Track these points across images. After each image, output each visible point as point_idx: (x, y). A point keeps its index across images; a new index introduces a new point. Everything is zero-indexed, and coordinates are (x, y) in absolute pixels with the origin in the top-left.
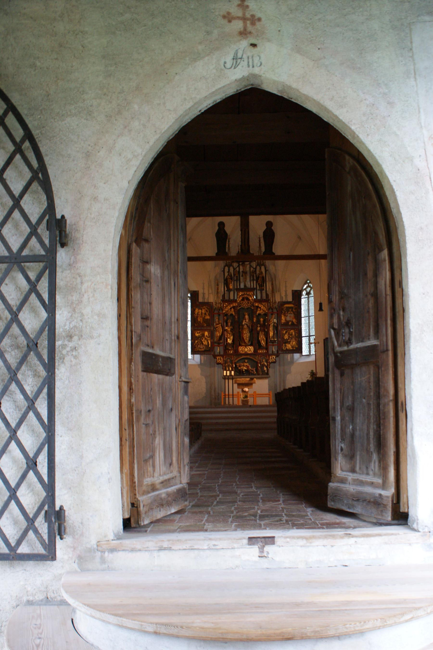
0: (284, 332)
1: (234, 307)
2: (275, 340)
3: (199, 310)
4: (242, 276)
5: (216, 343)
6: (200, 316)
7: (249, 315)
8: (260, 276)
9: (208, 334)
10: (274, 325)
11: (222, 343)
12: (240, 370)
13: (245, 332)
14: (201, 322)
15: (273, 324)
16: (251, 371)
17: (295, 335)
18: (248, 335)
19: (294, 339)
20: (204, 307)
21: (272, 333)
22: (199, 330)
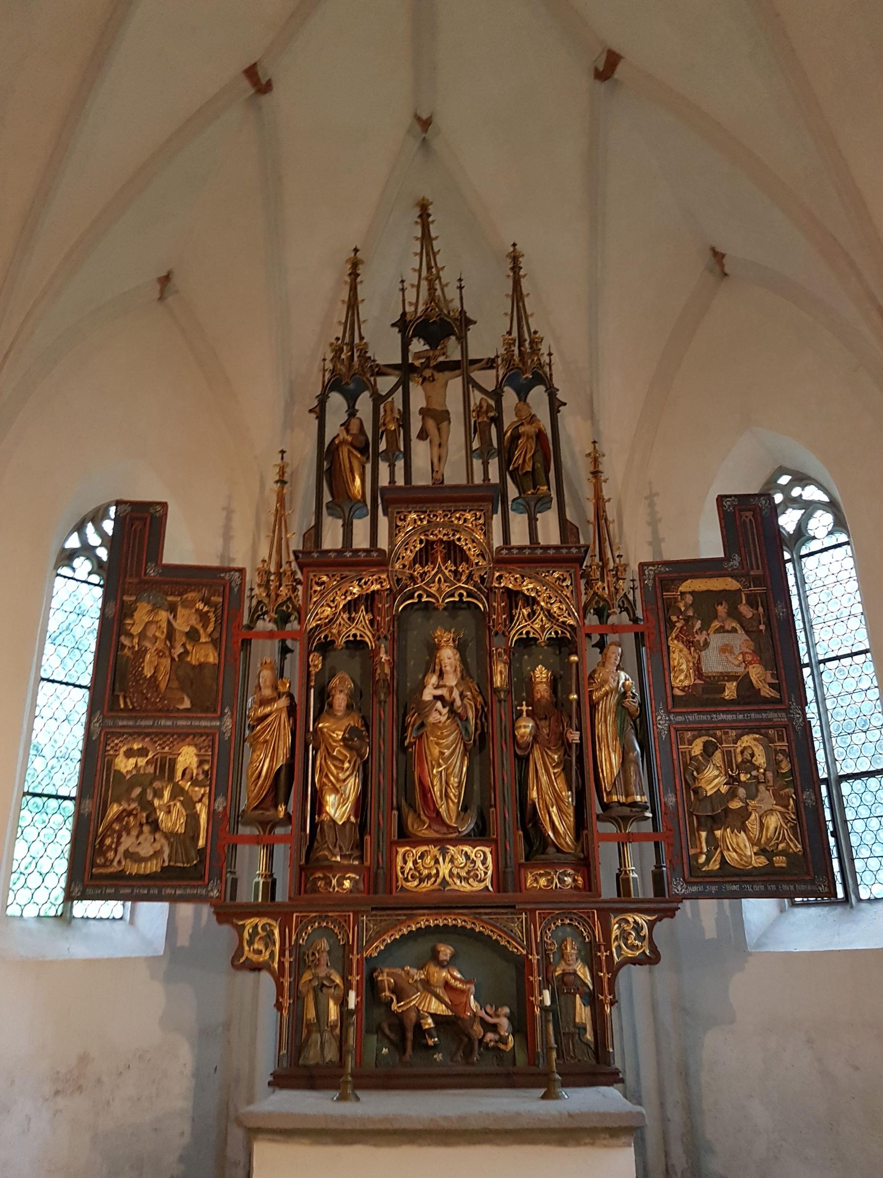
0: (697, 749)
1: (370, 600)
2: (634, 804)
3: (155, 608)
4: (423, 435)
5: (245, 824)
6: (159, 645)
7: (461, 647)
8: (522, 429)
9: (201, 763)
10: (620, 703)
11: (288, 817)
12: (398, 1022)
13: (436, 751)
14: (163, 686)
15: (613, 700)
16: (478, 1029)
17: (773, 764)
18: (459, 767)
19: (766, 799)
20: (190, 596)
21: (615, 759)
22: (141, 734)
